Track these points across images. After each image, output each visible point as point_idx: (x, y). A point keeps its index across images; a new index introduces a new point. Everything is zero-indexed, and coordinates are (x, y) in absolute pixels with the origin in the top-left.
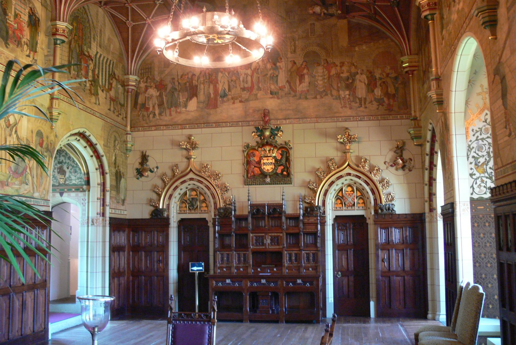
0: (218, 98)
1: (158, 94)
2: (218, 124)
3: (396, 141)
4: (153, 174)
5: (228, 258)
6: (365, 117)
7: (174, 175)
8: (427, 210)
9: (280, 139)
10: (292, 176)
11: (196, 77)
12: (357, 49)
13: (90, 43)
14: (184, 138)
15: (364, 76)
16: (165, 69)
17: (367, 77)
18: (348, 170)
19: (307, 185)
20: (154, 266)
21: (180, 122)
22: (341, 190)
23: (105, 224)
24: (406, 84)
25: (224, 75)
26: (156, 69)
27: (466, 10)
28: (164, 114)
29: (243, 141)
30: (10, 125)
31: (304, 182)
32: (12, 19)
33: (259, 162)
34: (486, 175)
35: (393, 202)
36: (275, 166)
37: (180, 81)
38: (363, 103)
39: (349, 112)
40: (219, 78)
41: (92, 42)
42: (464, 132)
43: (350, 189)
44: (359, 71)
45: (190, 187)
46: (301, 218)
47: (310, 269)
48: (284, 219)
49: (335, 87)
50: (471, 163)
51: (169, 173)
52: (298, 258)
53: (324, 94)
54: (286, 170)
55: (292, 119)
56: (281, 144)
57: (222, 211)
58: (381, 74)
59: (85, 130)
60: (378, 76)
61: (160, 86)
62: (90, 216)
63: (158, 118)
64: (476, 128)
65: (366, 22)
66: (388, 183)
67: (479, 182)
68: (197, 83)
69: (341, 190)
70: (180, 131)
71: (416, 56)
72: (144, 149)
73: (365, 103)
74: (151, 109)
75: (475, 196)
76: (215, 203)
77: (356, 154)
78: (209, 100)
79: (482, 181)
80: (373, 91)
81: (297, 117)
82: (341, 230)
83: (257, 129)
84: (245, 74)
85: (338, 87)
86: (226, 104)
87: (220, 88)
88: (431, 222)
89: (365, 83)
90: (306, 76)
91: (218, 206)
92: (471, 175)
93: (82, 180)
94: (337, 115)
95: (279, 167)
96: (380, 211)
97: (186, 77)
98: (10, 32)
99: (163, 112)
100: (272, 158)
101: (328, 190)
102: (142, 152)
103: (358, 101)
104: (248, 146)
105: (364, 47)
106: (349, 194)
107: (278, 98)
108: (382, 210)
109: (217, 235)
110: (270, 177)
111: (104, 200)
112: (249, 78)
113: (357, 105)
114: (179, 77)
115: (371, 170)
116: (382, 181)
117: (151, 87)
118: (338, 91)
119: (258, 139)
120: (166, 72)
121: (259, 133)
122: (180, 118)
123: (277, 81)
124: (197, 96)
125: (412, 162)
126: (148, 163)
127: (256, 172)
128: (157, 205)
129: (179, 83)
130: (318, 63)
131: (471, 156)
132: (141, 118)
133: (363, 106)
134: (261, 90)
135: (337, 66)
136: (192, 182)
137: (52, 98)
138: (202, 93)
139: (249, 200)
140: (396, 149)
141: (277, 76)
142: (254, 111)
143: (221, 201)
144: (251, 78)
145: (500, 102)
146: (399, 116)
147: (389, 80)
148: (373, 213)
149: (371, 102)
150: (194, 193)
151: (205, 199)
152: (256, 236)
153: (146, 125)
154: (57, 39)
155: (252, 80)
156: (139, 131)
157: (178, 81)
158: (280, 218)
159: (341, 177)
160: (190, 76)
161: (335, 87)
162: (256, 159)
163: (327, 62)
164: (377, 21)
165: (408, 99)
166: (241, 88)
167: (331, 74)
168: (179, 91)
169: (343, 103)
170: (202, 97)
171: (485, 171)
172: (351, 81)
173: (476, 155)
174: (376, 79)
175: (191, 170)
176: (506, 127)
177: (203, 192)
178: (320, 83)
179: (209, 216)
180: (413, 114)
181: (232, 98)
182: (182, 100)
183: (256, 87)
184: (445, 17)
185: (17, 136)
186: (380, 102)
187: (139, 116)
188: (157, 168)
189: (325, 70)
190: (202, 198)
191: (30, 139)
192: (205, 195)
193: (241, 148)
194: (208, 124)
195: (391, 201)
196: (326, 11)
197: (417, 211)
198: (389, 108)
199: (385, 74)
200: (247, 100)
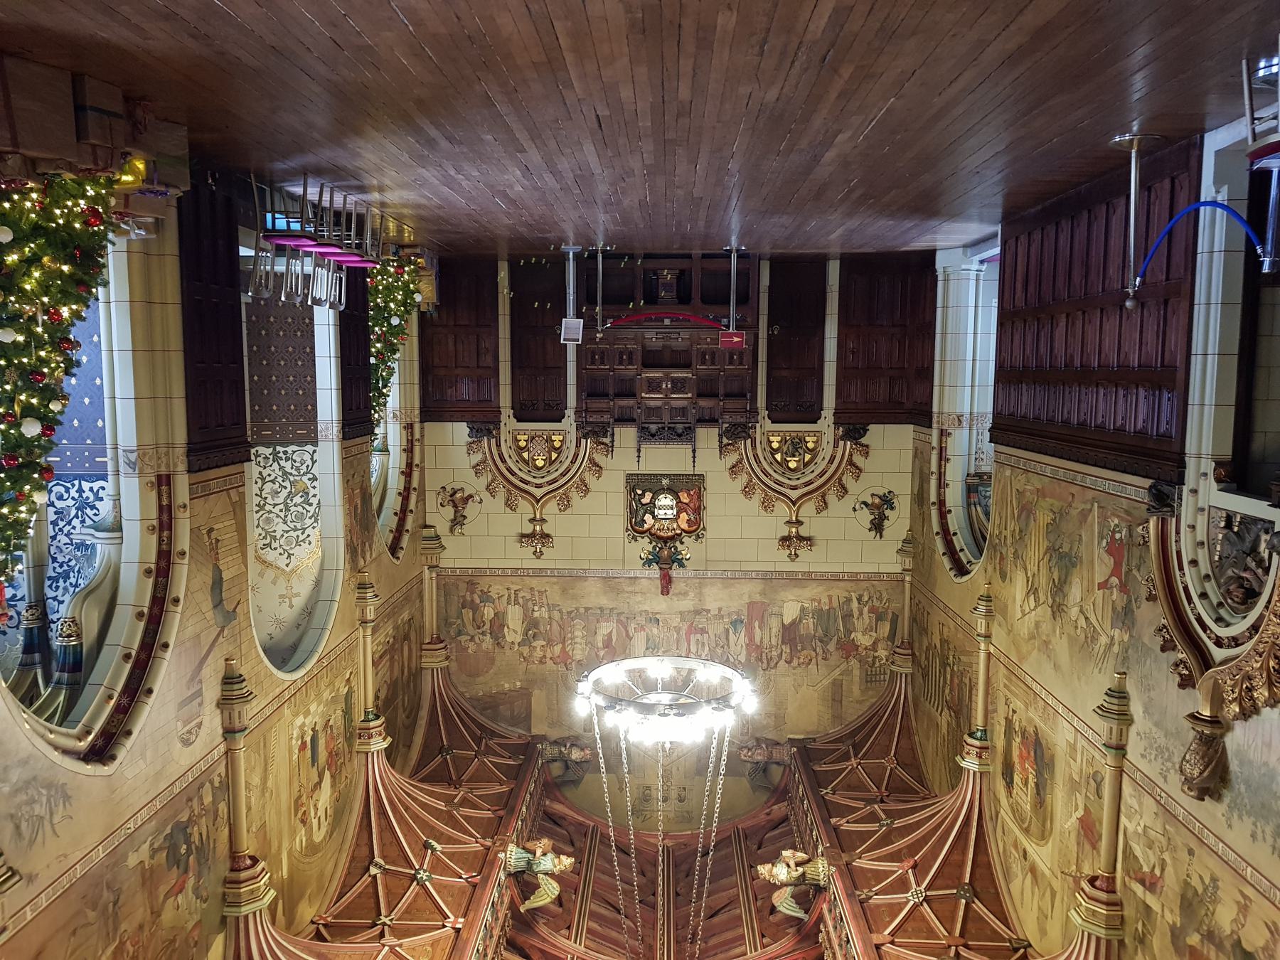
0: (746, 620)
1: (852, 636)
2: (747, 576)
4: (861, 499)
8: (417, 427)
9: (644, 546)
11: (784, 658)
12: (518, 684)
13: (948, 732)
15: (509, 639)
16: (841, 677)
21: (814, 584)
23: (938, 417)
24: (444, 621)
25: (736, 657)
26: (856, 679)
27: (287, 711)
28: (842, 600)
30: (1034, 593)
32: (1031, 776)
35: (470, 440)
36: (655, 505)
37: (813, 654)
38: (513, 596)
40: (744, 652)
41: (946, 733)
44: (516, 647)
49: (554, 624)
50: (314, 496)
51: (832, 498)
53: (573, 614)
54: (637, 497)
55: (626, 578)
56: (643, 538)
59: (954, 579)
60: (488, 635)
61: (849, 648)
62: (966, 432)
63: (853, 594)
65: (501, 727)
67: (304, 468)
68: (784, 647)
73: (509, 596)
74: (866, 609)
75: (310, 448)
76: (754, 447)
78: (763, 617)
79: (298, 469)
83: (681, 565)
85: (550, 625)
87: (743, 634)
89: (508, 628)
90: (600, 645)
91: (749, 441)
92: (315, 479)
93: (983, 493)
94: (555, 580)
95: (648, 501)
97: (801, 660)
98: (1032, 754)
99: (843, 603)
102: (881, 537)
103: (521, 601)
105: (507, 686)
106: (539, 455)
111: (940, 459)
113: (521, 594)
114: (814, 660)
118: (550, 618)
119: (680, 547)
120: (837, 671)
121: (680, 557)
122: (813, 590)
123: (648, 640)
125: (440, 501)
126: (873, 517)
127: (686, 495)
128: (854, 446)
129: (815, 650)
130: (581, 664)
131: (315, 506)
132: (885, 595)
133: (513, 592)
134: (675, 627)
135: (551, 659)
137: (988, 636)
138: (774, 630)
139: (694, 451)
140: (465, 522)
141: (647, 649)
142: (686, 594)
144: (690, 650)
146: (458, 573)
150: (792, 465)
151: (773, 455)
153: (874, 582)
154: (980, 739)
155: (689, 645)
157: (817, 655)
160: (795, 662)
161: (555, 626)
162: (684, 516)
163: (566, 665)
164: (481, 726)
166: (707, 633)
167: (560, 646)
169: (544, 598)
170: (775, 624)
172: (531, 632)
173: (307, 507)
174: (491, 634)
176: (217, 541)
178: (578, 633)
180: (434, 575)
181: (722, 617)
182: (809, 622)
183: (683, 633)
184: (339, 712)
185: (1027, 574)
186: (486, 598)
188: (855, 510)
189: (570, 654)
190: (778, 457)
191: (1014, 568)
192: (773, 461)
193: (708, 534)
194: (768, 578)
196: (563, 749)
198: (471, 585)
200: (697, 612)
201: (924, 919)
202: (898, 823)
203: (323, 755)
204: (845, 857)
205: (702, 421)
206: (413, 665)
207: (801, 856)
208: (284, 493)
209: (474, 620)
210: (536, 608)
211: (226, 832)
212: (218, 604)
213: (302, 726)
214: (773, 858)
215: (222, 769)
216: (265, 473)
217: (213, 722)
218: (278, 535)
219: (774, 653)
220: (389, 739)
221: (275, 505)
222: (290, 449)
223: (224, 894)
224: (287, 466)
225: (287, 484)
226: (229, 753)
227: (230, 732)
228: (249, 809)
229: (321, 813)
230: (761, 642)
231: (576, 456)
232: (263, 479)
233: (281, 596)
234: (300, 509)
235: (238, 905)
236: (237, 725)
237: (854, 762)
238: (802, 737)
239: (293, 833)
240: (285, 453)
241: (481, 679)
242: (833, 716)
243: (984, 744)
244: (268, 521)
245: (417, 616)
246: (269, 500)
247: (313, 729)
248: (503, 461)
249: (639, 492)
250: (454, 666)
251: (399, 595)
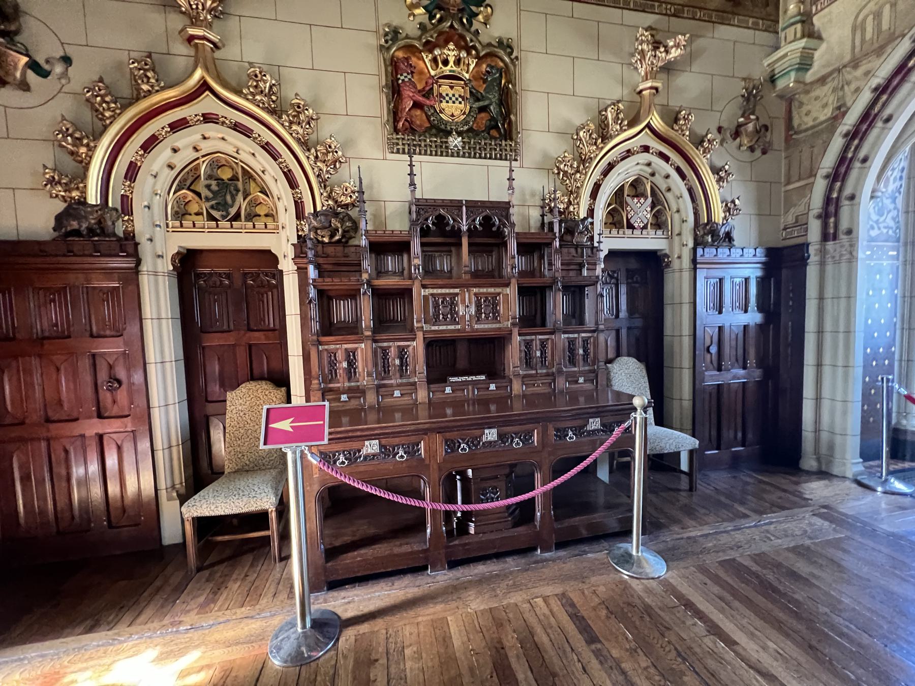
6: (686, 9)
29: (377, 19)
31: (546, 156)
91: (309, 209)
100: (463, 82)
101: (600, 185)
104: (394, 34)
109: (312, 293)
125: (769, 134)
146: (751, 21)
193: (374, 41)
205: (401, 247)
248: (690, 191)
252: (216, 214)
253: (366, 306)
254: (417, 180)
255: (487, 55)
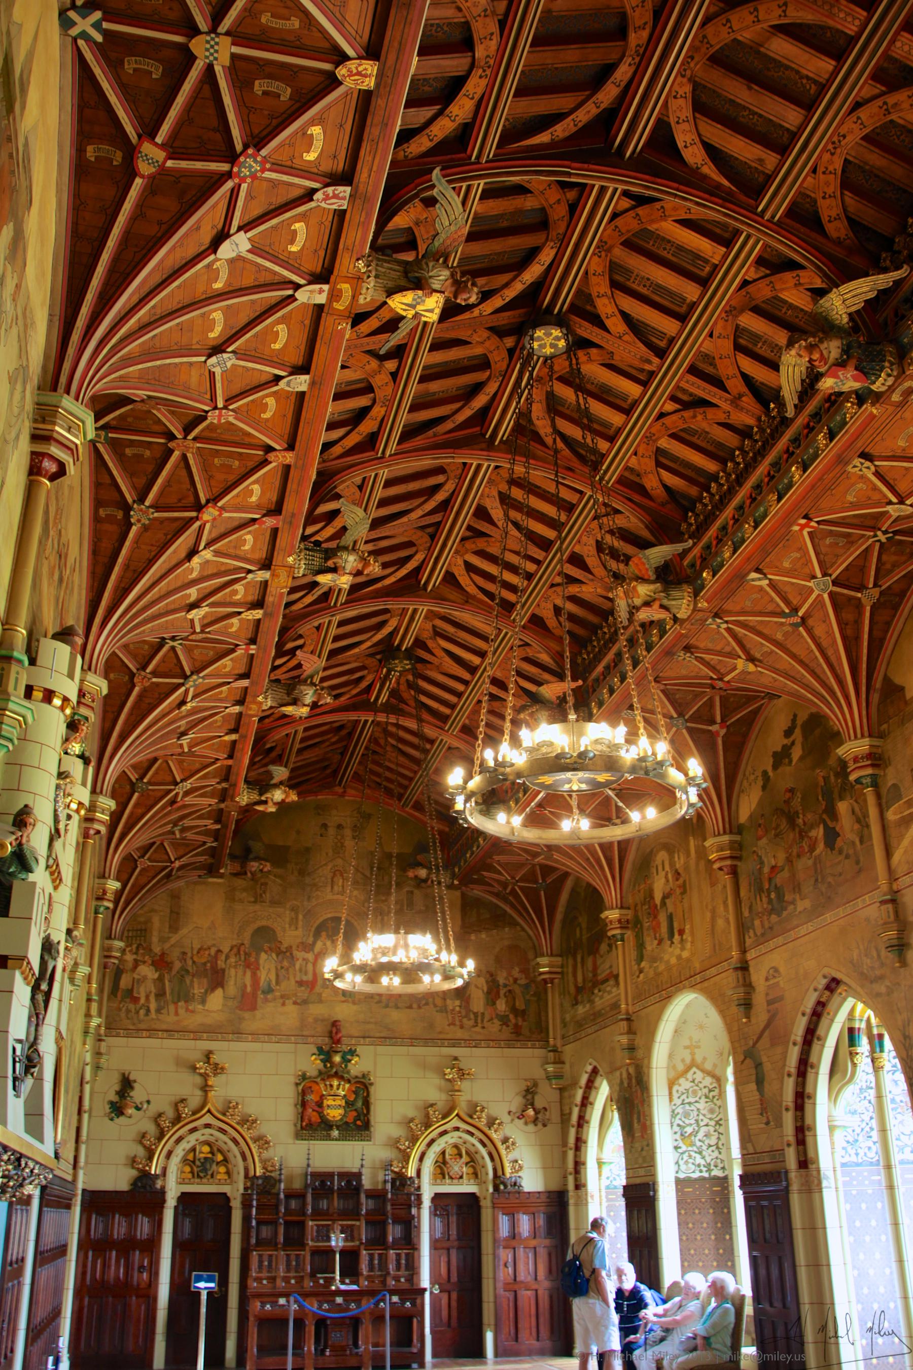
1: (156, 975)
2: (256, 1036)
3: (526, 1080)
4: (141, 1113)
5: (270, 1262)
7: (178, 1119)
8: (571, 1186)
9: (356, 1067)
10: (372, 1129)
14: (199, 1055)
17: (487, 982)
18: (456, 1122)
19: (394, 1143)
20: (132, 1277)
22: (443, 1153)
26: (155, 933)
27: (697, 966)
31: (390, 1138)
33: (320, 1104)
34: (695, 1149)
35: (520, 1174)
37: (195, 959)
39: (460, 1034)
40: (261, 962)
42: (667, 1093)
43: (455, 1151)
45: (202, 1138)
46: (389, 1196)
47: (403, 1280)
48: (363, 1197)
51: (170, 1113)
52: (383, 1260)
57: (260, 1182)
58: (506, 978)
60: (501, 981)
61: (161, 963)
64: (681, 1089)
66: (513, 1144)
67: (685, 1157)
68: (223, 966)
69: (443, 1153)
70: (191, 1043)
71: (559, 959)
72: (126, 1067)
73: (482, 1021)
74: (142, 1001)
75: (682, 1176)
77: (469, 1097)
79: (690, 1156)
80: (494, 1004)
81: (382, 1035)
82: (441, 1216)
83: (320, 1050)
84: (304, 959)
86: (272, 1004)
88: (577, 1204)
91: (252, 1173)
92: (676, 1148)
96: (502, 1187)
102: (124, 1074)
103: (472, 1016)
104: (304, 1077)
107: (354, 1003)
108: (506, 1186)
110: (338, 1128)
112: (310, 967)
113: (472, 1023)
114: (195, 952)
115: (491, 1124)
116: (505, 1140)
117: (144, 962)
119: (321, 1066)
122: (193, 1021)
124: (223, 987)
126: (132, 1094)
129: (194, 962)
132: (123, 1015)
136: (208, 1131)
139: (308, 1165)
142: (316, 1020)
143: (258, 1164)
145: (753, 1086)
147: (517, 990)
148: (491, 1190)
149: (492, 1019)
150: (206, 1149)
152: (317, 1225)
156: (117, 1036)
158: (358, 1194)
159: (444, 1133)
160: (213, 951)
165: (543, 1018)
168: (193, 976)
170: (232, 988)
171: (692, 1144)
175: (209, 1111)
176: (761, 1114)
177: (224, 1147)
179: (235, 1190)
181: (282, 997)
182: (197, 990)
184: (649, 948)
186: (504, 1021)
187: (120, 1009)
188: (148, 1102)
190: (220, 1157)
193: (293, 1080)
194: (237, 1034)
195: (517, 1171)
197: (554, 1187)
198: (517, 1031)
199: (511, 979)
200: (305, 1002)
201: (183, 770)
202: (170, 826)
203: (662, 918)
204: (222, 806)
205: (301, 1196)
206: (571, 961)
207: (260, 808)
208: (700, 1135)
209: (514, 998)
210: (458, 1009)
211: (743, 893)
212: (758, 1065)
213: (683, 949)
214: (281, 804)
215: (748, 942)
216: (716, 1154)
217: (758, 977)
218: (703, 1100)
219: (232, 960)
220: (603, 916)
221: (707, 1125)
222: (696, 1175)
223: (741, 850)
224: (699, 1160)
225: (698, 1144)
226: (744, 951)
227: (744, 968)
228: (725, 903)
229: (662, 874)
230: (245, 973)
231: (421, 1159)
232: (718, 1148)
233: (698, 1047)
234: (687, 1121)
235: (732, 842)
236: (740, 973)
237: (177, 864)
238: (211, 880)
239: (686, 868)
240: (701, 1171)
241: (506, 943)
242: (179, 898)
243: (99, 903)
244: (712, 1111)
245: (567, 1004)
246: (712, 1129)
247: (673, 943)
249: (359, 1123)
250: (531, 955)
251: (589, 1031)
252: (202, 1175)
253: (281, 1230)
254: (311, 1162)
255: (356, 1082)
